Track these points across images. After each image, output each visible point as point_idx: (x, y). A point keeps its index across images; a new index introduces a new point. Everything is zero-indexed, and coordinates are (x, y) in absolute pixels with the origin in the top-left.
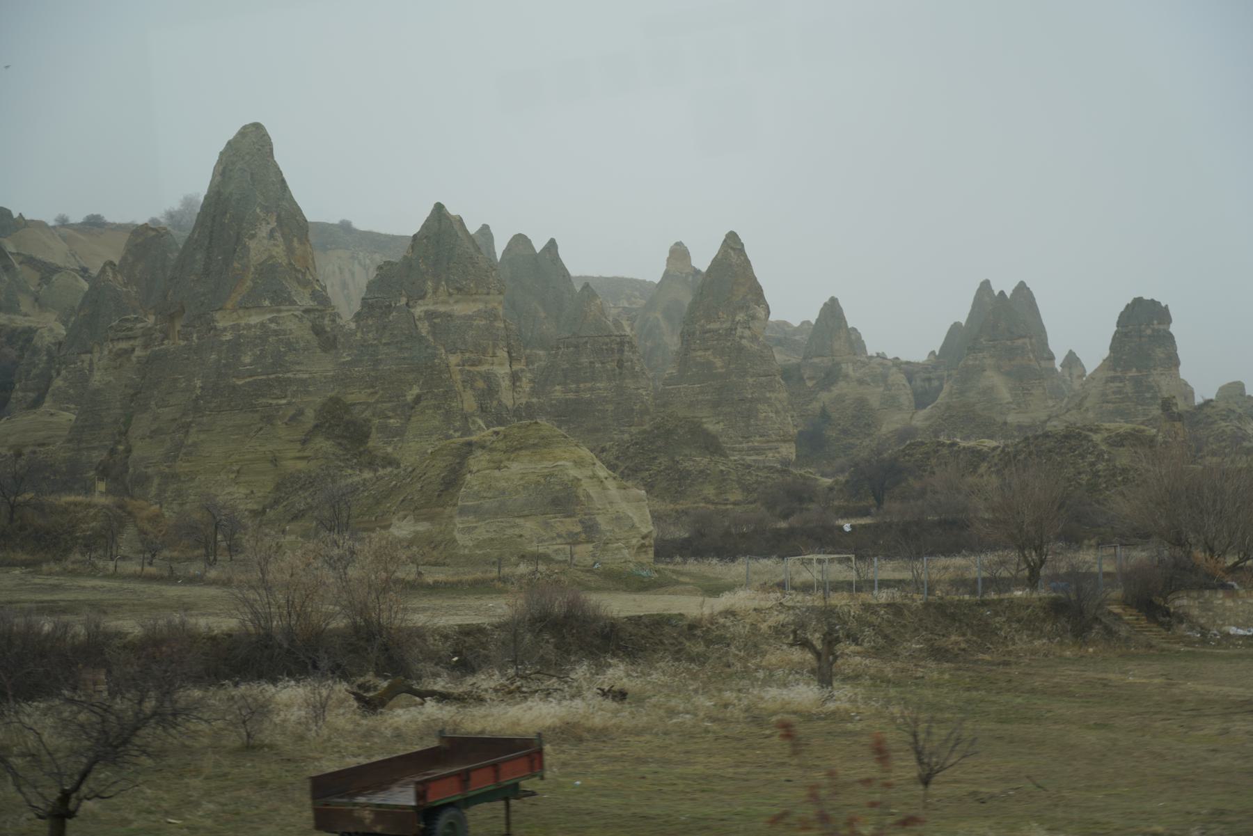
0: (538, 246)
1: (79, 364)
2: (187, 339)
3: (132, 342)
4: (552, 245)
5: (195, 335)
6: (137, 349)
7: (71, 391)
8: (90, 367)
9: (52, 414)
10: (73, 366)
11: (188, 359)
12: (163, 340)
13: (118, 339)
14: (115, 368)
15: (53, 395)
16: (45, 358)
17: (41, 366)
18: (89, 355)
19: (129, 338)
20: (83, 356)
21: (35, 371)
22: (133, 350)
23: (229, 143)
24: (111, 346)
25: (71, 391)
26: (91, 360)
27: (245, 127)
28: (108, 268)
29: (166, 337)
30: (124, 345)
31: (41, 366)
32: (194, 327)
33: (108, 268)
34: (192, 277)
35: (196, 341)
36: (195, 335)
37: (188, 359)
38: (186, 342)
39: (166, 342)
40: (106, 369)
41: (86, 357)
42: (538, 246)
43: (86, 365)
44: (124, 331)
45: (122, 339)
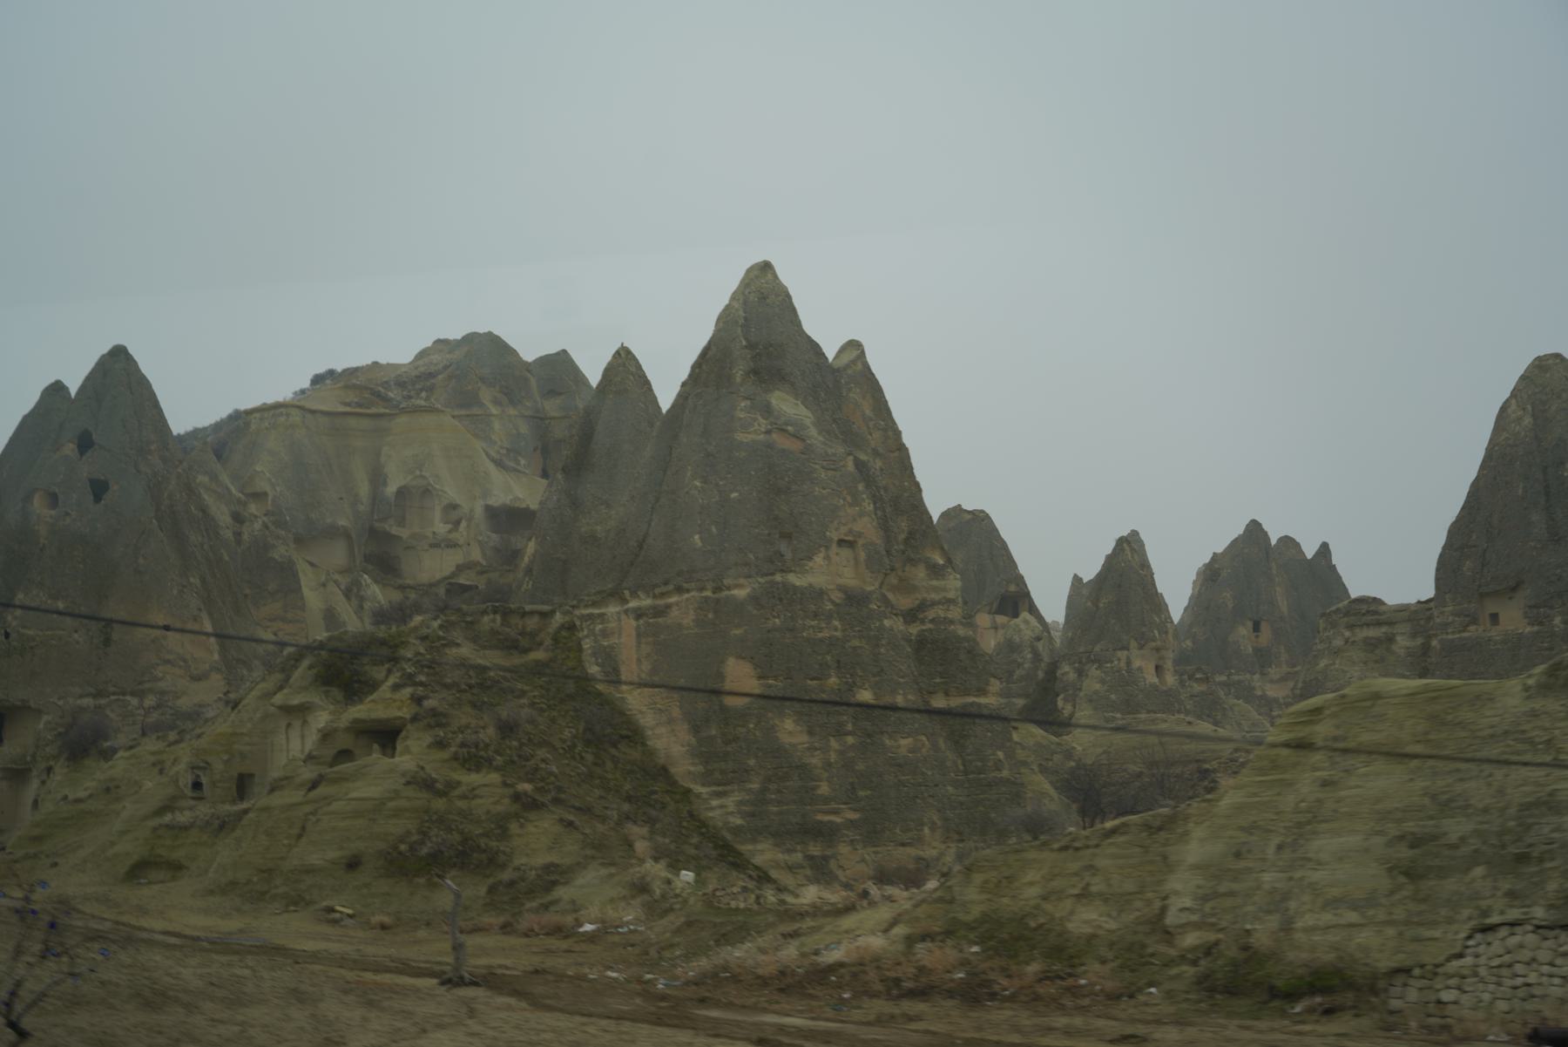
0: (1310, 551)
1: (1116, 662)
2: (1541, 623)
3: (1384, 629)
4: (1324, 550)
5: (1558, 620)
6: (1399, 638)
7: (1113, 697)
8: (1128, 667)
9: (1189, 723)
10: (1109, 665)
11: (1551, 649)
12: (1467, 626)
13: (1361, 626)
14: (1376, 662)
15: (1091, 701)
16: (1029, 656)
17: (1026, 666)
18: (1126, 652)
19: (1379, 624)
20: (1119, 653)
21: (1018, 673)
22: (1390, 639)
23: (1523, 378)
24: (1347, 634)
25: (1113, 697)
26: (1128, 658)
27: (1539, 358)
28: (1125, 545)
29: (1474, 621)
30: (1372, 633)
31: (1026, 666)
32: (1551, 608)
33: (1125, 545)
34: (1533, 544)
35: (1562, 626)
36: (1558, 620)
37: (1551, 649)
38: (1536, 628)
39: (1472, 628)
40: (1365, 663)
41: (1122, 654)
42: (1310, 551)
43: (1123, 664)
44: (1364, 614)
45: (1368, 625)
